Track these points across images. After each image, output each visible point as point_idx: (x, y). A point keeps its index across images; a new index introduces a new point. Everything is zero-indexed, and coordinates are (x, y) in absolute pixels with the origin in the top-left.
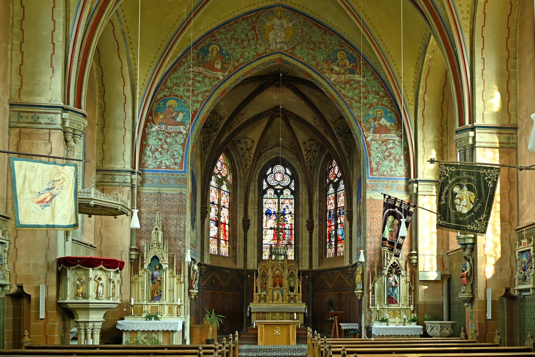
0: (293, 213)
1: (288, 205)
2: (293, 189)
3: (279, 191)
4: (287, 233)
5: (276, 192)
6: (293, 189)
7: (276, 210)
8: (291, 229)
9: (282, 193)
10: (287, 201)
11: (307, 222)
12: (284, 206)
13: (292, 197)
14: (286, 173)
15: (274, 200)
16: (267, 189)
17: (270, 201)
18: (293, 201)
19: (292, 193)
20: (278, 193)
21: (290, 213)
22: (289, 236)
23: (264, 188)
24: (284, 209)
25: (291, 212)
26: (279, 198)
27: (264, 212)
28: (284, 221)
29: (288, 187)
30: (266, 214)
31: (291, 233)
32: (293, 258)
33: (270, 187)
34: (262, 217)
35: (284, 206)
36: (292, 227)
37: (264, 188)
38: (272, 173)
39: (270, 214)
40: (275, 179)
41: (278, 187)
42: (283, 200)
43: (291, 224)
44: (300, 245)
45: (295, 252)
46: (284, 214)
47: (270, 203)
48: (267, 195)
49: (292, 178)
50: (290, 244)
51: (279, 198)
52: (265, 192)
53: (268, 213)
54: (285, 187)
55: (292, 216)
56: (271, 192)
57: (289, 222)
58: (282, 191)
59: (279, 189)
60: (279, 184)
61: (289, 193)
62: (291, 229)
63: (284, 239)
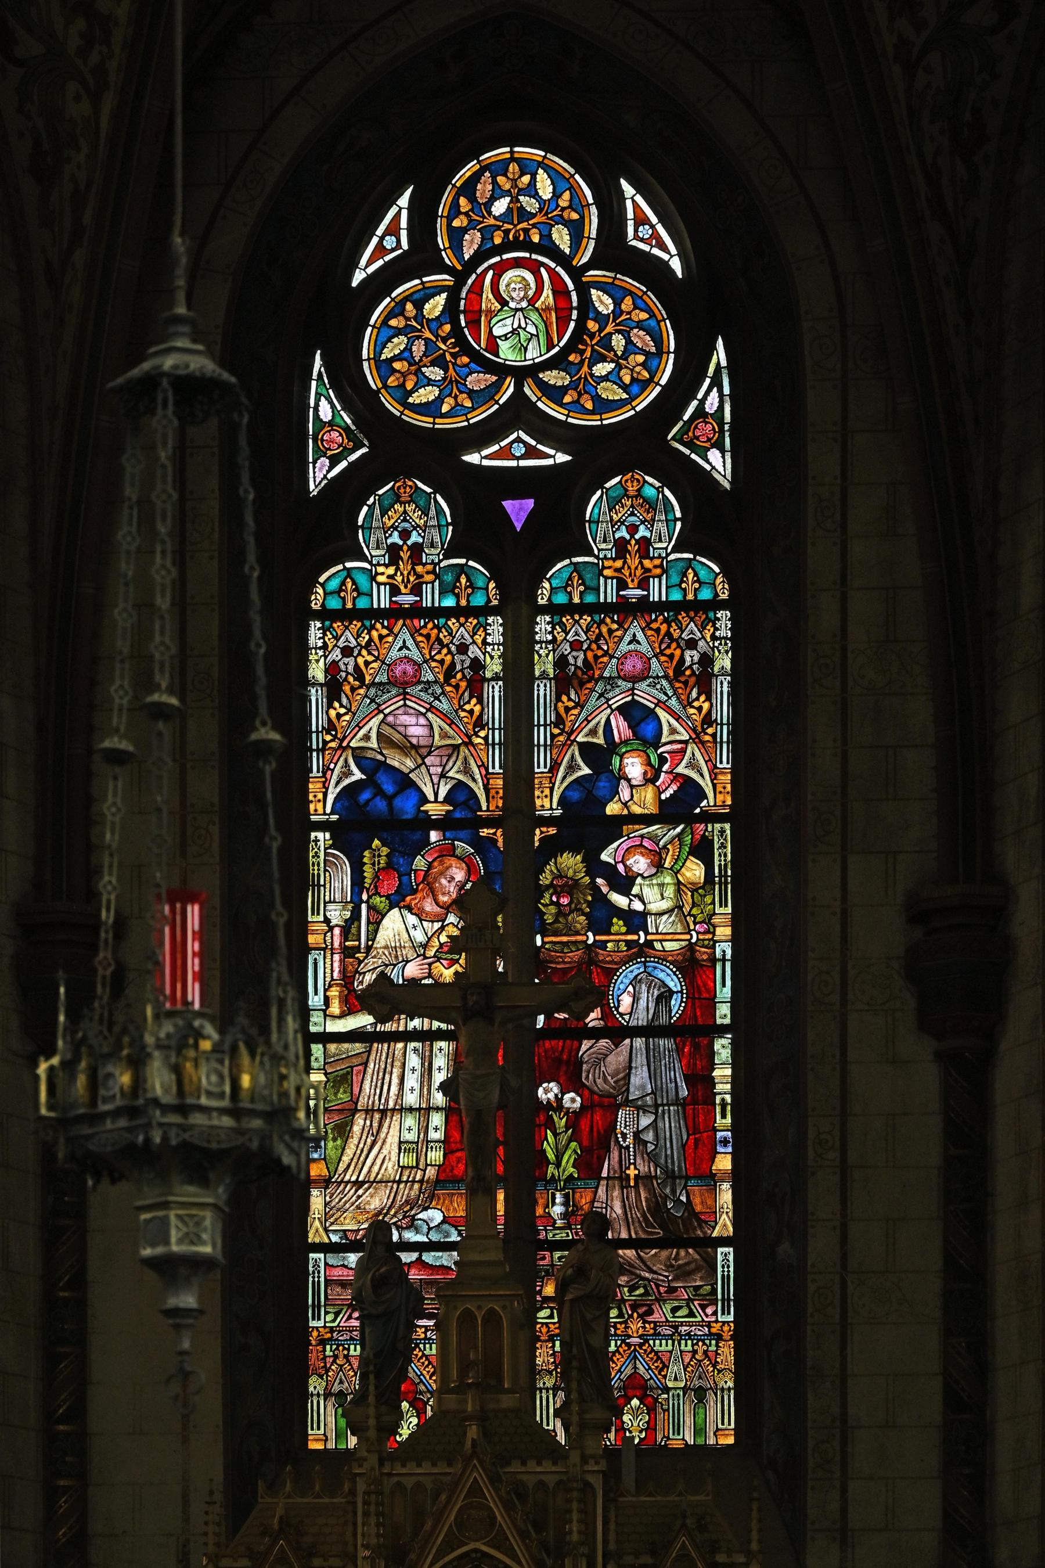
0: (717, 795)
1: (645, 695)
2: (718, 463)
3: (518, 510)
4: (640, 1078)
5: (478, 528)
6: (718, 463)
7: (484, 772)
8: (693, 1033)
9: (560, 528)
10: (636, 639)
11: (918, 913)
12: (602, 717)
13: (709, 577)
14: (614, 251)
15: (460, 630)
16: (351, 489)
17: (402, 645)
18: (717, 641)
19: (709, 520)
20: (516, 539)
21: (681, 806)
22: (672, 1124)
23: (319, 474)
24: (600, 756)
25: (690, 790)
26: (517, 605)
27: (323, 802)
28: (602, 915)
29: (643, 445)
30: (352, 831)
31: (701, 1080)
32: (719, 1425)
33: (397, 451)
34: (299, 883)
35: (602, 717)
36: (701, 998)
37: (319, 474)
38: (421, 257)
39: (407, 833)
40: (462, 338)
41: (513, 453)
42: (578, 629)
43: (693, 966)
44: (821, 1245)
45: (743, 1336)
46: (587, 823)
47: (391, 694)
48: (368, 575)
49: (696, 309)
50: (678, 1231)
51: (517, 605)
52: (328, 529)
53: (382, 822)
54: (600, 454)
55: (703, 850)
56: (405, 528)
57: (668, 934)
58: (560, 509)
59: (518, 482)
60: (519, 414)
61: (664, 535)
62: (693, 1033)
63: (589, 1167)
